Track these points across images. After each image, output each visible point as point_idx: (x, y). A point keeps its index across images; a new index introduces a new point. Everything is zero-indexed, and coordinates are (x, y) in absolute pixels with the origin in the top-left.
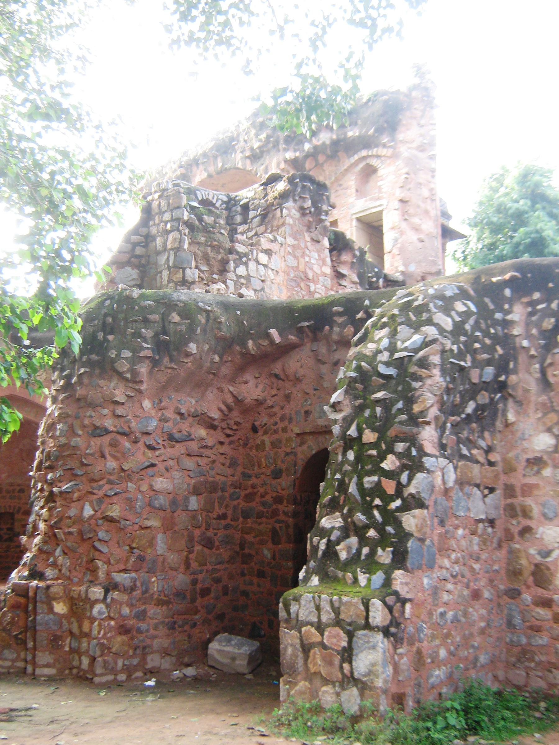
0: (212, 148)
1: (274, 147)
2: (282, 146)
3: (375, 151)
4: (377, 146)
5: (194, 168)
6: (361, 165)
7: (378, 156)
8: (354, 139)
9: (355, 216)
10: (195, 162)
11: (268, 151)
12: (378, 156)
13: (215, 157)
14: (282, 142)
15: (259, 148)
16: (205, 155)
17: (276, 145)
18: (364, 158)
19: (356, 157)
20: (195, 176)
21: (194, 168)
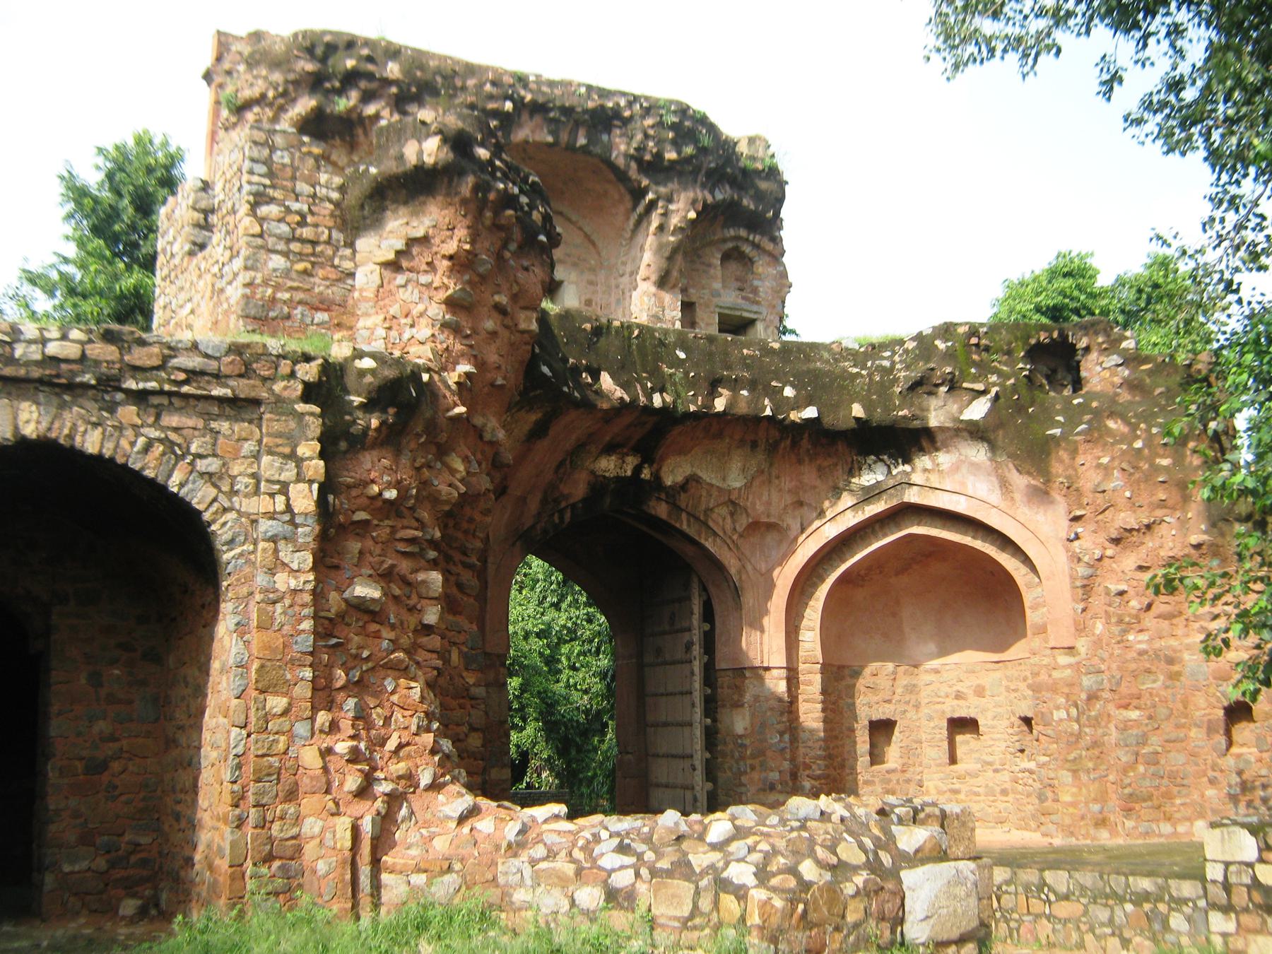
0: (586, 111)
1: (691, 173)
2: (701, 178)
3: (758, 238)
4: (763, 234)
5: (525, 116)
6: (730, 245)
7: (756, 246)
8: (747, 210)
9: (718, 310)
10: (538, 108)
11: (681, 174)
12: (756, 246)
13: (577, 124)
14: (703, 172)
15: (672, 162)
16: (568, 111)
17: (696, 172)
18: (738, 238)
19: (732, 232)
20: (520, 126)
21: (525, 116)
